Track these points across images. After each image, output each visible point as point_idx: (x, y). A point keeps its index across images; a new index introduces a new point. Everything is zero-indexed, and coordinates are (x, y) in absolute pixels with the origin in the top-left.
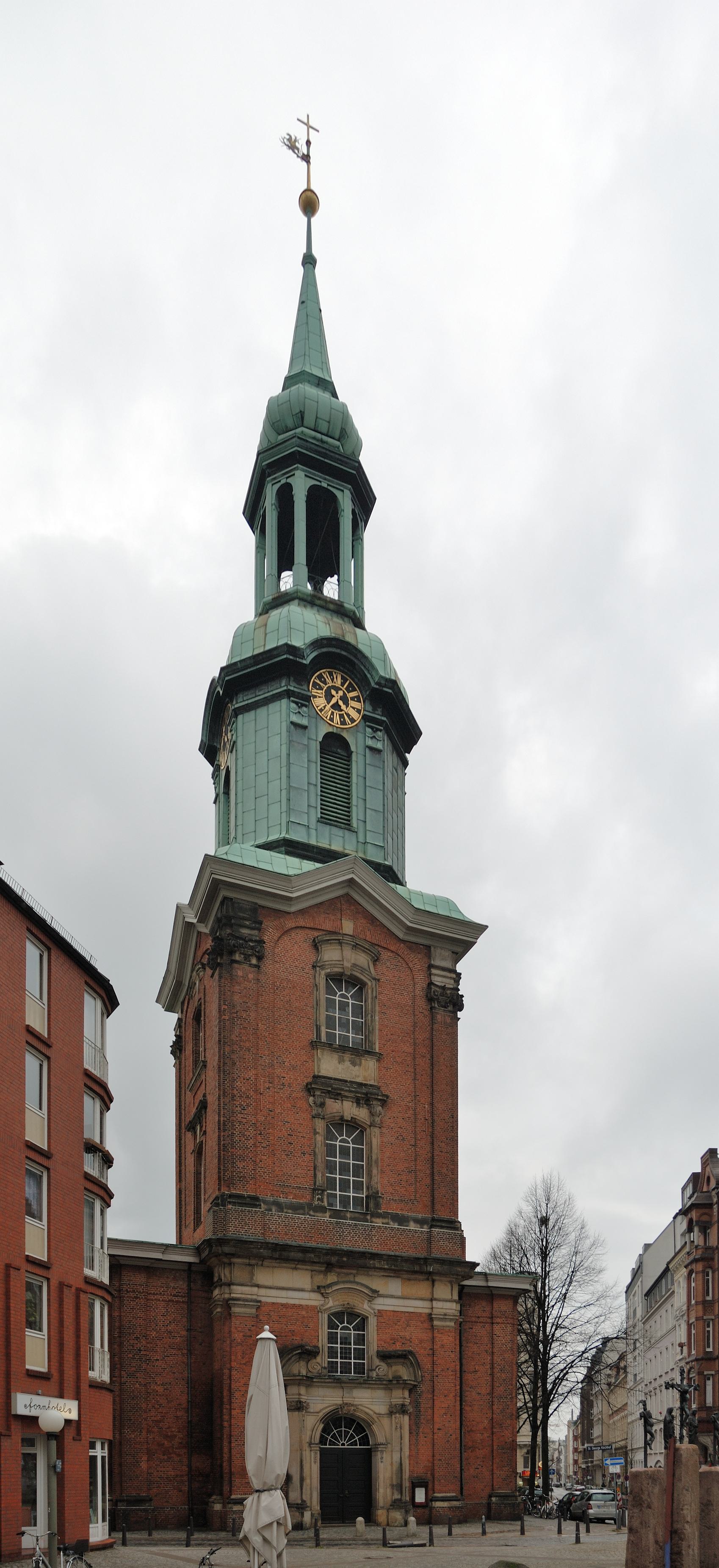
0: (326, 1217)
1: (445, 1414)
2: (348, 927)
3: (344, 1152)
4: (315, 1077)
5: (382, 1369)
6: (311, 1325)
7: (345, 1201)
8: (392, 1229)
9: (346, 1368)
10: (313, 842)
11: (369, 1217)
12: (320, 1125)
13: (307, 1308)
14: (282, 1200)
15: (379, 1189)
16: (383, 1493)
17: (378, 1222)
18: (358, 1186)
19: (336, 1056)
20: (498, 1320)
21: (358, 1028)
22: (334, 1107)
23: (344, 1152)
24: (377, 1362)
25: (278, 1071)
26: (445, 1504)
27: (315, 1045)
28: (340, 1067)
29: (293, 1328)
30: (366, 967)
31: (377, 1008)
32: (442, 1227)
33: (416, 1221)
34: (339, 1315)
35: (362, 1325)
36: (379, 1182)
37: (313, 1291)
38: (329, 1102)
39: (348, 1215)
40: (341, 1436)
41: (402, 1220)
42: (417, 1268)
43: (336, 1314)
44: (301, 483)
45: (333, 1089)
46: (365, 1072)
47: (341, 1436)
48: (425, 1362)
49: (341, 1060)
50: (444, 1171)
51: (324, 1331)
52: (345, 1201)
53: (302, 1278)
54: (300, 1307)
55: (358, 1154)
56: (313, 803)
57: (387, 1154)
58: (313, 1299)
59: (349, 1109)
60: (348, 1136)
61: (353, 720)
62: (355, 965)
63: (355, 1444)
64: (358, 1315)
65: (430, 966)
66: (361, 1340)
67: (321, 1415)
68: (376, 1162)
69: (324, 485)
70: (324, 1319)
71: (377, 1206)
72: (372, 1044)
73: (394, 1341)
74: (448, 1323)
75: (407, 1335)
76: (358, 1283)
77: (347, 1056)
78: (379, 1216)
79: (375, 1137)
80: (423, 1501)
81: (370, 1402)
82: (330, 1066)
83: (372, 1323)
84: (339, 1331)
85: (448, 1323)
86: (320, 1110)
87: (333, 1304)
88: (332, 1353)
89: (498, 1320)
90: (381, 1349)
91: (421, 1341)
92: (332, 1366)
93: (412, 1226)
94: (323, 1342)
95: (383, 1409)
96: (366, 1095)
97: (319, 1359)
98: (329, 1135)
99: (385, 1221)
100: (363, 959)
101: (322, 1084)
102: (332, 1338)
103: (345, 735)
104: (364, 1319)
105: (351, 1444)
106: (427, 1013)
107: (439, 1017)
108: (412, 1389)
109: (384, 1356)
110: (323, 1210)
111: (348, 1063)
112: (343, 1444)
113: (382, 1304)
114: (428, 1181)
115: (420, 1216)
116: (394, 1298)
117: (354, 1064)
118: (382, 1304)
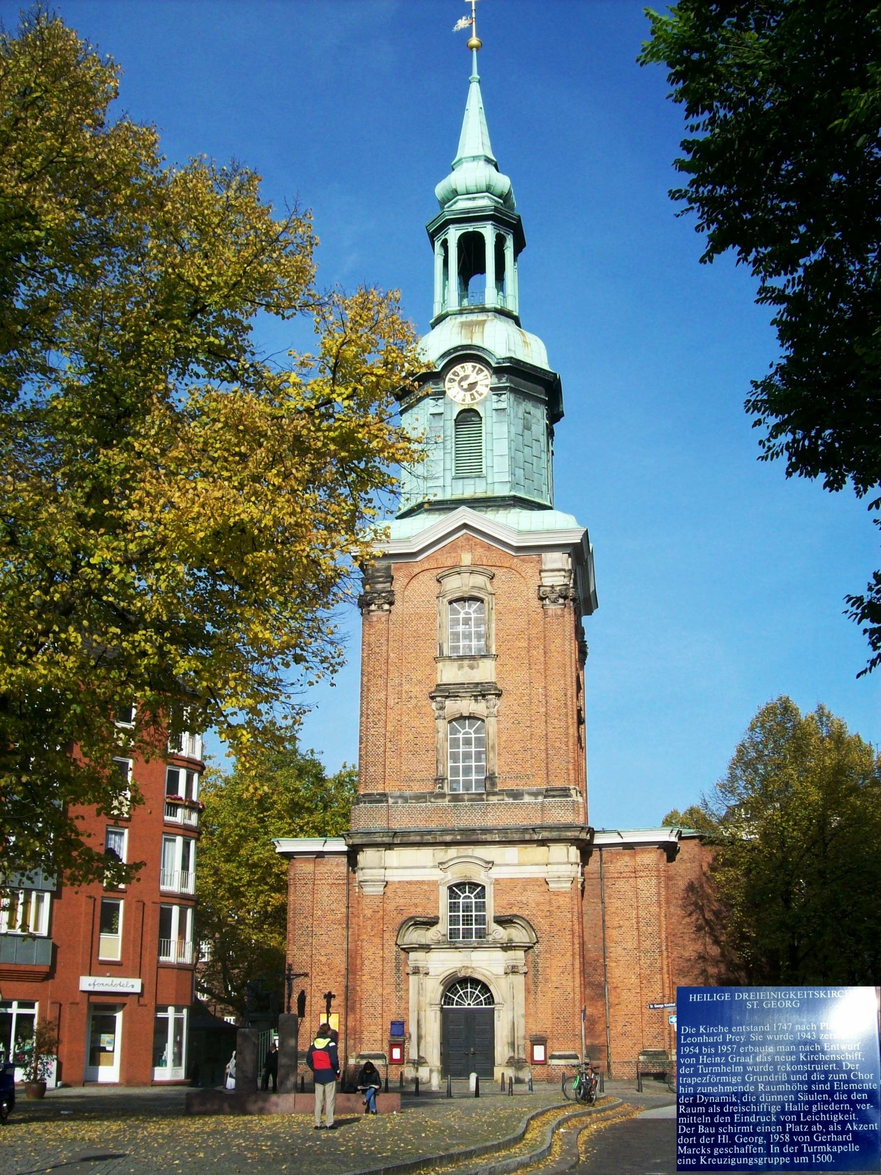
0: (445, 802)
1: (563, 972)
2: (466, 559)
3: (467, 742)
4: (438, 685)
5: (499, 933)
6: (432, 898)
7: (467, 785)
8: (506, 804)
9: (467, 934)
10: (448, 497)
11: (485, 797)
12: (442, 725)
13: (429, 883)
14: (408, 793)
15: (496, 771)
16: (501, 1052)
17: (494, 799)
18: (479, 770)
19: (456, 664)
20: (642, 874)
21: (479, 636)
22: (453, 707)
23: (467, 742)
24: (494, 926)
25: (406, 687)
26: (562, 1062)
27: (441, 657)
28: (460, 672)
29: (416, 901)
30: (482, 585)
31: (494, 617)
32: (554, 796)
33: (531, 794)
34: (461, 886)
35: (482, 895)
36: (496, 764)
37: (434, 867)
38: (448, 703)
39: (466, 797)
40: (467, 997)
41: (516, 795)
42: (527, 837)
43: (457, 885)
44: (453, 235)
45: (447, 692)
46: (485, 672)
47: (467, 997)
48: (536, 921)
49: (461, 667)
50: (557, 744)
51: (444, 900)
52: (467, 785)
53: (425, 855)
54: (422, 882)
55: (480, 742)
56: (448, 466)
57: (504, 738)
58: (436, 875)
59: (466, 706)
60: (470, 727)
61: (481, 395)
62: (473, 587)
63: (481, 1003)
64: (478, 885)
65: (541, 571)
66: (481, 907)
67: (441, 978)
68: (493, 747)
69: (471, 229)
70: (444, 893)
71: (494, 784)
72: (488, 647)
73: (511, 905)
74: (564, 885)
75: (524, 899)
76: (471, 857)
77: (466, 662)
78: (495, 794)
79: (492, 725)
80: (542, 1058)
81: (487, 964)
82: (449, 674)
83: (489, 891)
84: (461, 900)
85: (564, 885)
86: (441, 712)
87: (453, 876)
88: (453, 920)
89: (642, 874)
90: (498, 914)
91: (538, 904)
92: (453, 933)
93: (527, 799)
94: (443, 912)
95: (501, 971)
96: (481, 691)
97: (438, 927)
98: (454, 731)
99: (500, 797)
100: (480, 580)
101: (440, 691)
102: (453, 907)
103: (475, 407)
104: (484, 887)
105: (477, 1004)
106: (540, 610)
107: (550, 612)
108: (528, 949)
109: (502, 921)
110: (443, 796)
111: (466, 669)
112: (469, 1004)
113: (496, 873)
114: (544, 755)
115: (534, 789)
116: (509, 864)
117: (472, 667)
118: (496, 873)
